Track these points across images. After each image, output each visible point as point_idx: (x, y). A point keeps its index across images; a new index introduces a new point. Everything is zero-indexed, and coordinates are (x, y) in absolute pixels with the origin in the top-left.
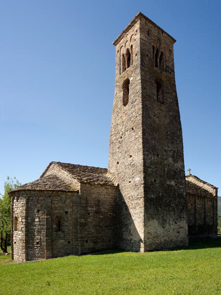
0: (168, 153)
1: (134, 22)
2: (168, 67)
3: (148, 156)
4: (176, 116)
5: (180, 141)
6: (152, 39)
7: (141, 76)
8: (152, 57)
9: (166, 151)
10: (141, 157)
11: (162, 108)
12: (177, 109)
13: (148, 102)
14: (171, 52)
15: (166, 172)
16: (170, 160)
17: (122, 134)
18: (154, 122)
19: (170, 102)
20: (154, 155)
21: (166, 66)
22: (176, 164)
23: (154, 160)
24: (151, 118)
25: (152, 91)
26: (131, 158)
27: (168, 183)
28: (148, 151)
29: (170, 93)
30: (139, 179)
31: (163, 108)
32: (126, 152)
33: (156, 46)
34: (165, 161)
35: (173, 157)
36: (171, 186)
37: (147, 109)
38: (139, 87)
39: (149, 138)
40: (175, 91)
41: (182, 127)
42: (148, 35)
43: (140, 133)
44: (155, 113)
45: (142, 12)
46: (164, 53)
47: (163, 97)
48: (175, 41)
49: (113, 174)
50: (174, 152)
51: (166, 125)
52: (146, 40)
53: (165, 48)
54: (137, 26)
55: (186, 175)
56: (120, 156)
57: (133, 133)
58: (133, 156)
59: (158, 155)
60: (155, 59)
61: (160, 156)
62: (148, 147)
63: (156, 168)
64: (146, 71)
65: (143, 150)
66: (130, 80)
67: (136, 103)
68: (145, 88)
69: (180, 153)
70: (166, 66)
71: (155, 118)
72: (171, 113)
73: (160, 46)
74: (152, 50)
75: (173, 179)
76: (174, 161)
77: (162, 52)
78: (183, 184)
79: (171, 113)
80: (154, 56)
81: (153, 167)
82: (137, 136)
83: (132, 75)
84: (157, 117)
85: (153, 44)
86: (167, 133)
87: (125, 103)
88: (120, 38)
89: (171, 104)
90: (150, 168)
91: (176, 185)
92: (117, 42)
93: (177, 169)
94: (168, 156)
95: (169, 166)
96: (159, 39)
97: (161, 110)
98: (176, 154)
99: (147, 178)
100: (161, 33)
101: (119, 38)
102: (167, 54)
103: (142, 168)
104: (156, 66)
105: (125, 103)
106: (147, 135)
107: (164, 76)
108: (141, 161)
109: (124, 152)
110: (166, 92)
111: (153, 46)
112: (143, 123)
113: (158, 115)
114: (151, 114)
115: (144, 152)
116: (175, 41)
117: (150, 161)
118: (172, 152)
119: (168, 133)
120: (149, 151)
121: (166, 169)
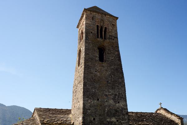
0: (109, 96)
2: (111, 36)
3: (88, 101)
4: (119, 68)
5: (121, 86)
6: (95, 21)
7: (86, 46)
8: (96, 32)
9: (106, 95)
10: (82, 102)
11: (104, 65)
12: (119, 63)
13: (90, 63)
14: (114, 26)
15: (106, 111)
16: (111, 102)
18: (96, 75)
19: (112, 60)
20: (94, 99)
21: (109, 35)
22: (117, 104)
23: (93, 103)
24: (92, 73)
25: (94, 55)
27: (108, 120)
29: (112, 53)
30: (81, 119)
31: (104, 64)
33: (100, 25)
34: (106, 103)
35: (114, 99)
36: (112, 122)
37: (88, 68)
40: (118, 51)
41: (124, 75)
42: (93, 20)
44: (96, 69)
46: (107, 27)
47: (106, 57)
48: (117, 18)
49: (73, 115)
50: (116, 95)
51: (107, 76)
52: (91, 23)
53: (108, 24)
55: (128, 111)
58: (80, 102)
59: (98, 100)
60: (99, 33)
61: (99, 100)
62: (87, 94)
63: (95, 109)
64: (90, 43)
68: (88, 54)
69: (122, 95)
70: (109, 35)
71: (96, 73)
72: (113, 67)
73: (103, 24)
74: (96, 28)
75: (114, 116)
76: (115, 102)
77: (106, 28)
78: (126, 119)
79: (113, 67)
80: (99, 31)
81: (92, 109)
84: (98, 72)
85: (97, 24)
86: (108, 82)
87: (79, 66)
89: (112, 61)
90: (90, 110)
91: (117, 121)
93: (118, 108)
94: (108, 99)
95: (110, 106)
96: (102, 20)
97: (103, 66)
98: (117, 97)
99: (86, 118)
100: (104, 16)
102: (110, 28)
103: (82, 110)
104: (101, 37)
105: (79, 66)
106: (87, 86)
107: (106, 43)
110: (108, 53)
111: (98, 26)
113: (99, 71)
114: (92, 71)
115: (84, 98)
116: (117, 18)
117: (89, 105)
118: (113, 95)
119: (109, 82)
120: (89, 97)
121: (106, 109)
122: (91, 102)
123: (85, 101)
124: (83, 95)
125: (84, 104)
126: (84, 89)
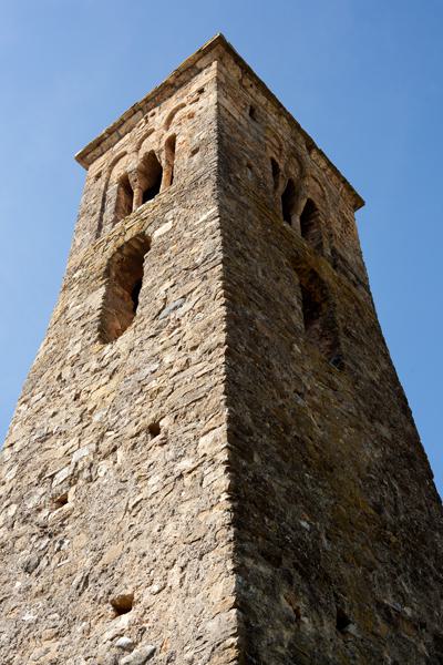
1: (189, 71)
3: (271, 592)
7: (221, 208)
17: (73, 479)
26: (125, 619)
28: (273, 560)
32: (86, 581)
38: (208, 244)
39: (279, 485)
43: (214, 442)
45: (229, 39)
54: (207, 77)
56: (29, 617)
57: (158, 454)
65: (237, 538)
66: (157, 234)
67: (187, 306)
82: (186, 464)
83: (169, 216)
88: (115, 131)
92: (98, 151)
101: (110, 132)
108: (221, 622)
109: (62, 592)
112: (234, 390)
115: (239, 551)
117: (287, 635)
122: (298, 616)
123: (256, 585)
124: (235, 523)
125: (242, 605)
126: (231, 467)
